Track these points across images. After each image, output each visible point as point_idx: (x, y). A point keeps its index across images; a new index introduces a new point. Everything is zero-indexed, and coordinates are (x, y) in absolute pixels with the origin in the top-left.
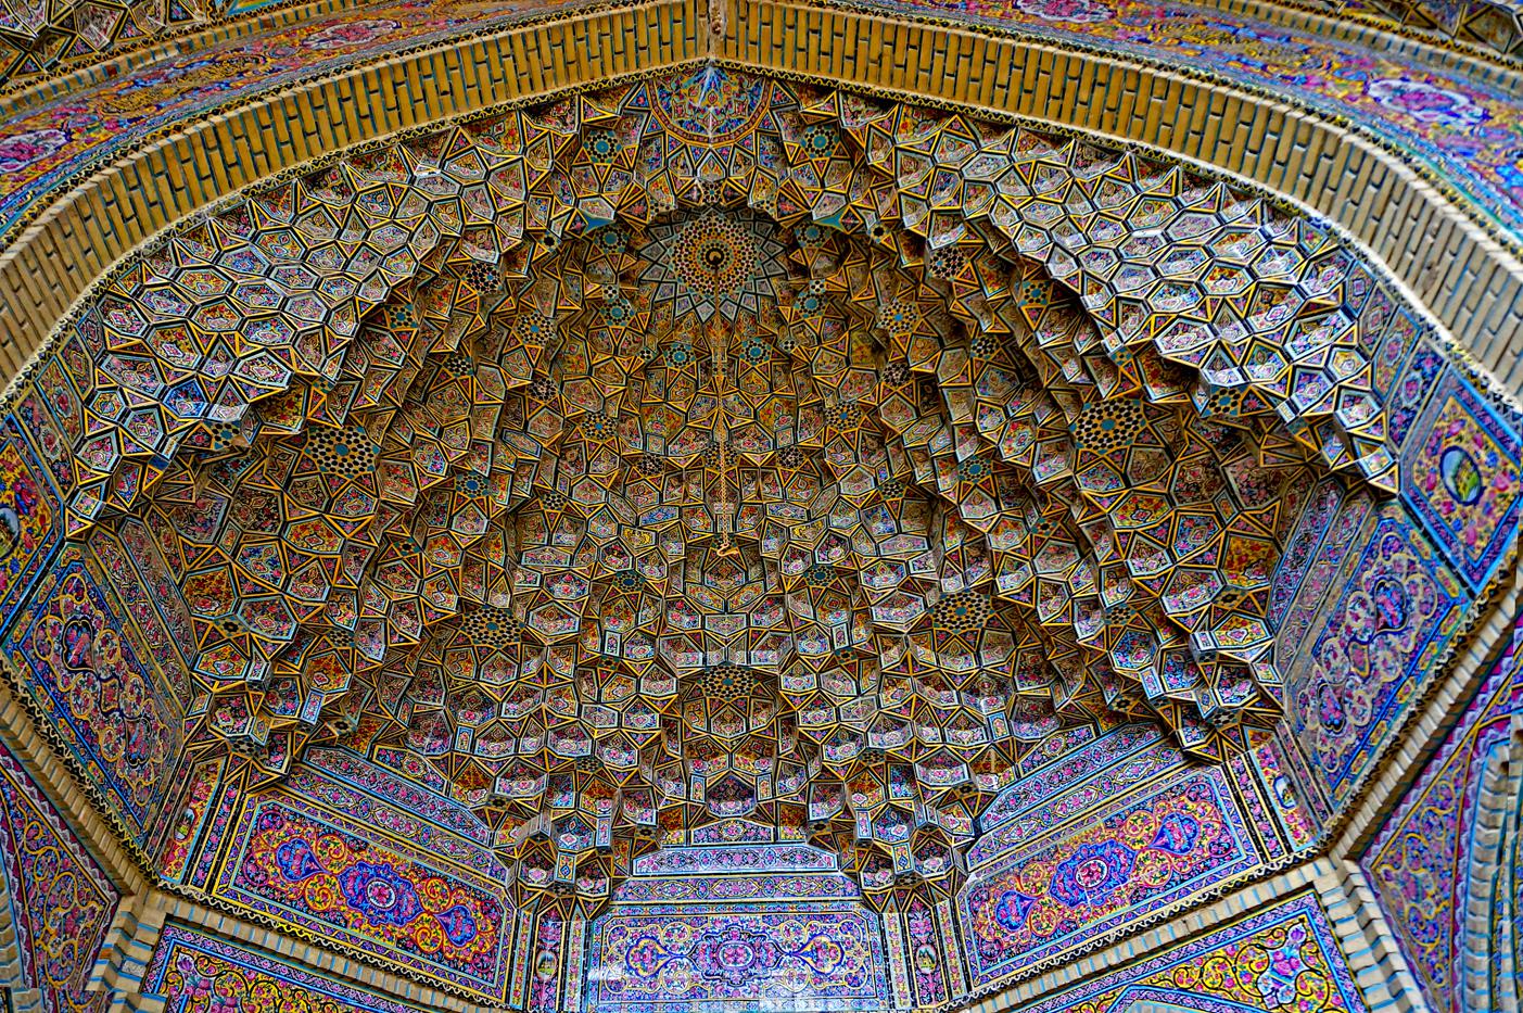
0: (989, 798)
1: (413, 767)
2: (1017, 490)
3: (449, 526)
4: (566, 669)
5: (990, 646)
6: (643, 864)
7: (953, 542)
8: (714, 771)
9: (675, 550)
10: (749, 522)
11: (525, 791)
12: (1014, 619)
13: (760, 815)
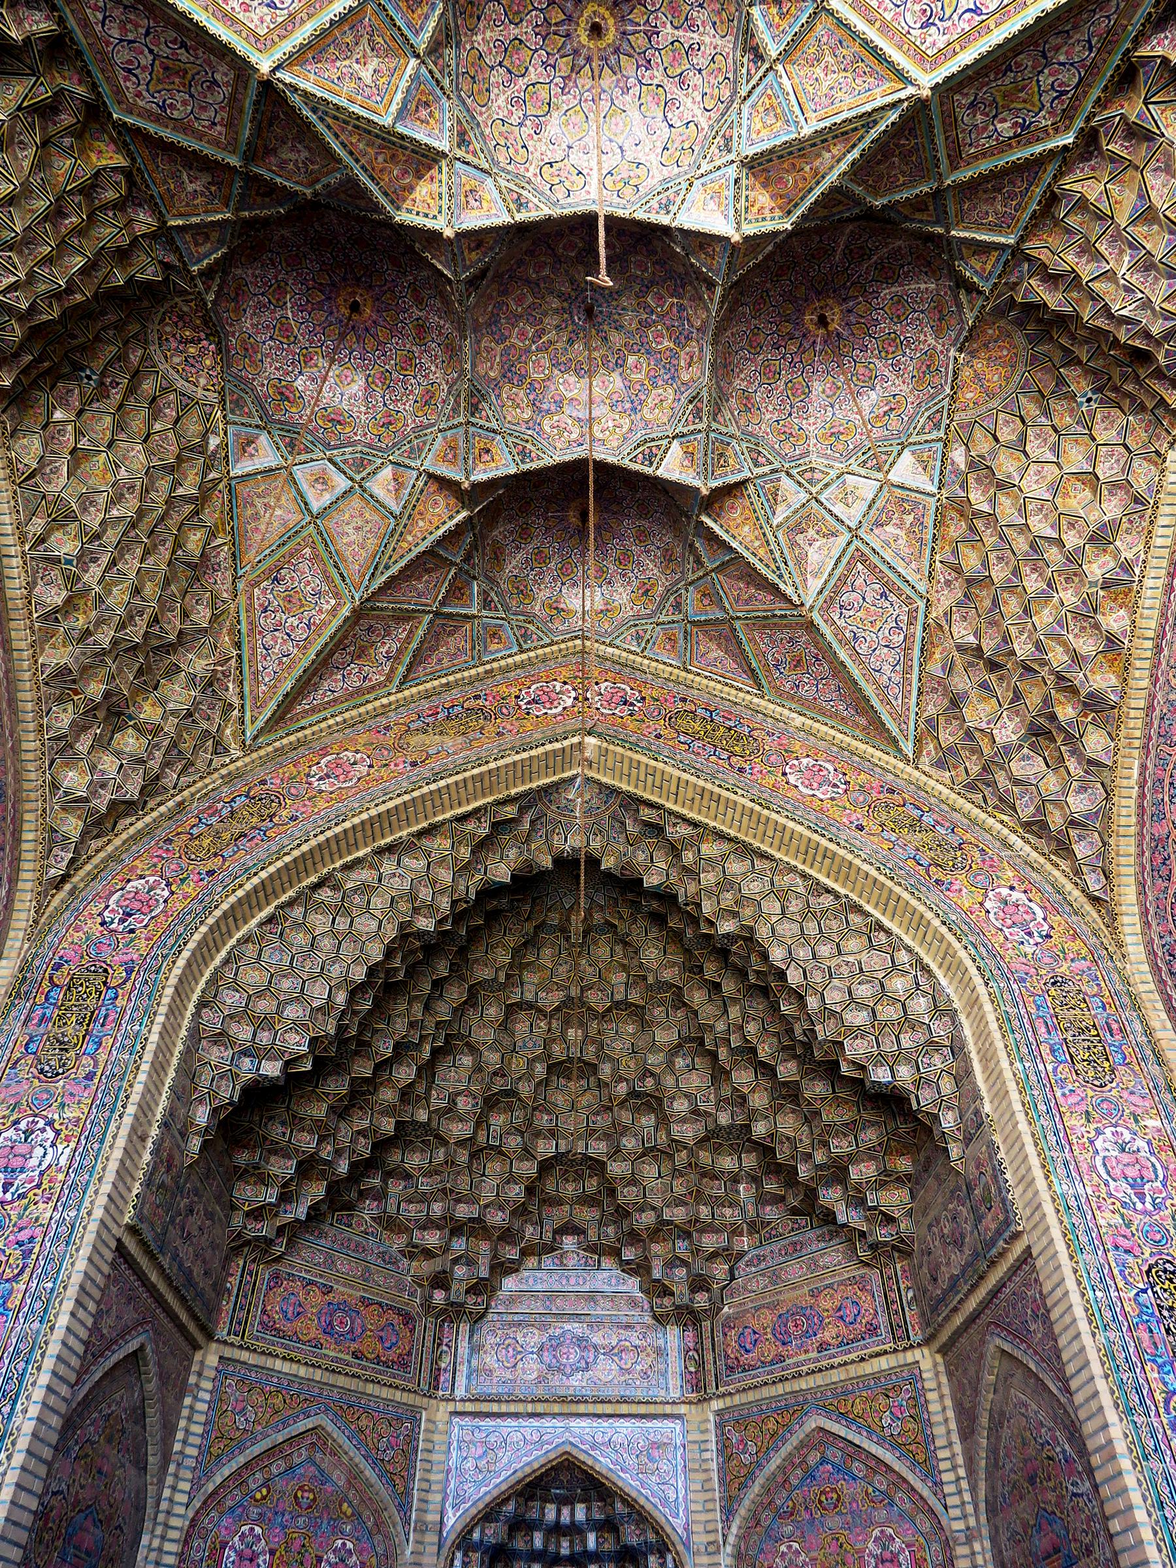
0: (741, 1255)
1: (359, 1224)
2: (766, 1070)
4: (463, 1156)
5: (748, 1152)
6: (510, 1284)
7: (726, 1091)
8: (558, 1216)
9: (540, 1069)
10: (592, 1048)
11: (432, 1239)
12: (765, 1150)
13: (592, 1249)
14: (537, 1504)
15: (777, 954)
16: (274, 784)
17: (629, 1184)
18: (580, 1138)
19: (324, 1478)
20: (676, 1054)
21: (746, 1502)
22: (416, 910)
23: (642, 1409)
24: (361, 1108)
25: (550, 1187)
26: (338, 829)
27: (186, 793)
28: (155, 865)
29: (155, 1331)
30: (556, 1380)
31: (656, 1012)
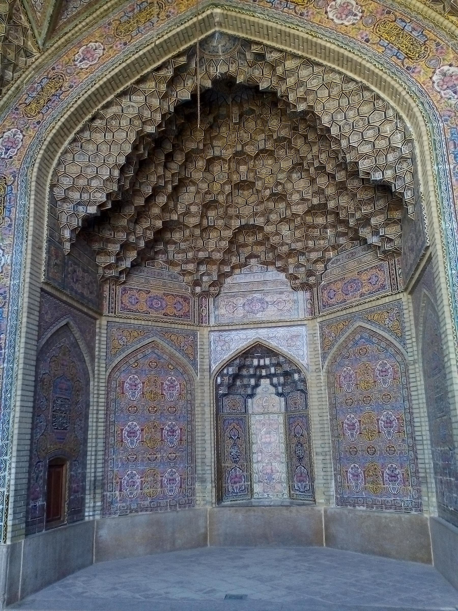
0: (329, 260)
2: (332, 176)
3: (155, 200)
4: (197, 232)
8: (247, 251)
9: (228, 188)
11: (191, 267)
14: (250, 359)
15: (326, 120)
16: (59, 69)
17: (275, 235)
18: (250, 217)
19: (159, 357)
20: (292, 172)
21: (331, 354)
22: (144, 123)
23: (288, 324)
24: (145, 218)
25: (241, 239)
26: (93, 89)
27: (19, 82)
28: (13, 123)
29: (73, 317)
30: (250, 316)
31: (281, 153)
